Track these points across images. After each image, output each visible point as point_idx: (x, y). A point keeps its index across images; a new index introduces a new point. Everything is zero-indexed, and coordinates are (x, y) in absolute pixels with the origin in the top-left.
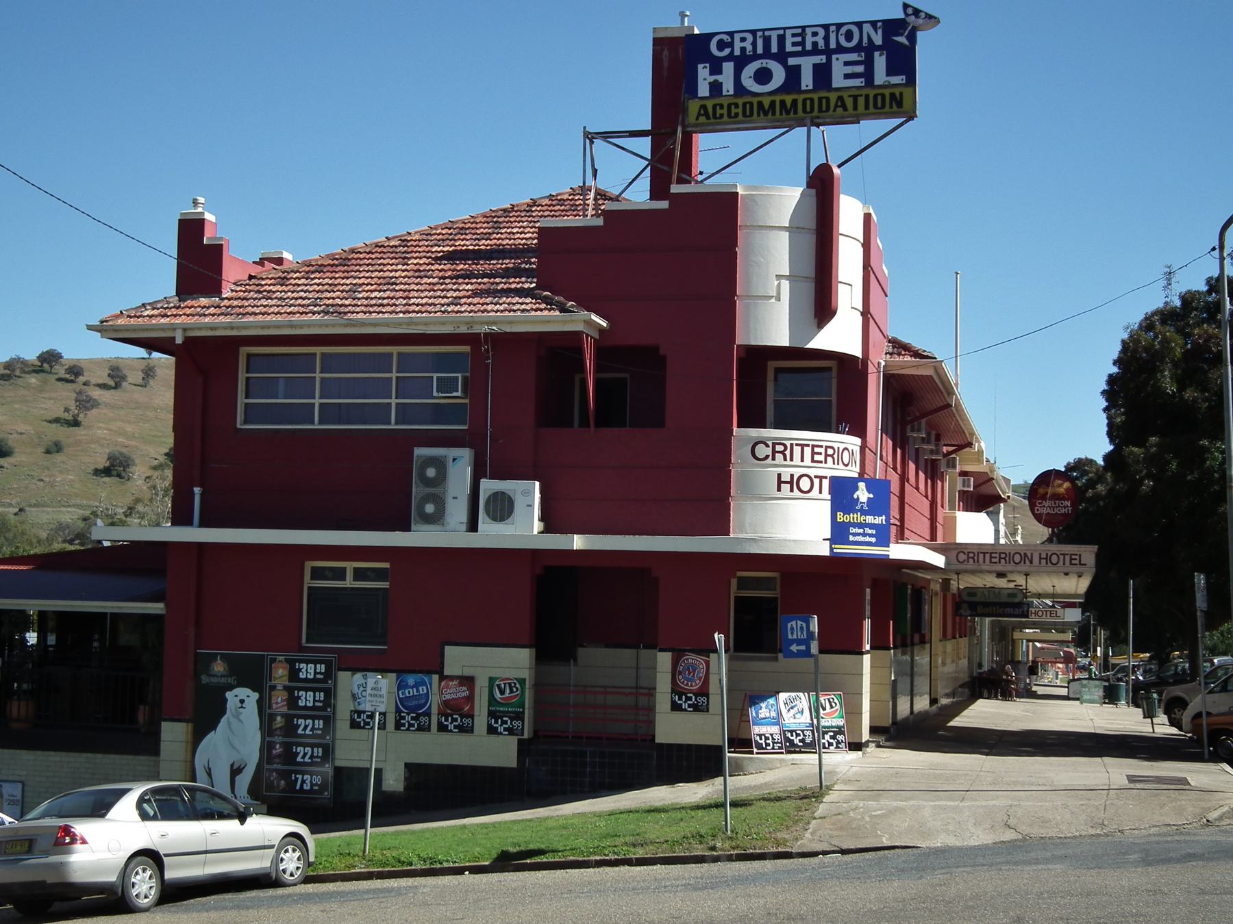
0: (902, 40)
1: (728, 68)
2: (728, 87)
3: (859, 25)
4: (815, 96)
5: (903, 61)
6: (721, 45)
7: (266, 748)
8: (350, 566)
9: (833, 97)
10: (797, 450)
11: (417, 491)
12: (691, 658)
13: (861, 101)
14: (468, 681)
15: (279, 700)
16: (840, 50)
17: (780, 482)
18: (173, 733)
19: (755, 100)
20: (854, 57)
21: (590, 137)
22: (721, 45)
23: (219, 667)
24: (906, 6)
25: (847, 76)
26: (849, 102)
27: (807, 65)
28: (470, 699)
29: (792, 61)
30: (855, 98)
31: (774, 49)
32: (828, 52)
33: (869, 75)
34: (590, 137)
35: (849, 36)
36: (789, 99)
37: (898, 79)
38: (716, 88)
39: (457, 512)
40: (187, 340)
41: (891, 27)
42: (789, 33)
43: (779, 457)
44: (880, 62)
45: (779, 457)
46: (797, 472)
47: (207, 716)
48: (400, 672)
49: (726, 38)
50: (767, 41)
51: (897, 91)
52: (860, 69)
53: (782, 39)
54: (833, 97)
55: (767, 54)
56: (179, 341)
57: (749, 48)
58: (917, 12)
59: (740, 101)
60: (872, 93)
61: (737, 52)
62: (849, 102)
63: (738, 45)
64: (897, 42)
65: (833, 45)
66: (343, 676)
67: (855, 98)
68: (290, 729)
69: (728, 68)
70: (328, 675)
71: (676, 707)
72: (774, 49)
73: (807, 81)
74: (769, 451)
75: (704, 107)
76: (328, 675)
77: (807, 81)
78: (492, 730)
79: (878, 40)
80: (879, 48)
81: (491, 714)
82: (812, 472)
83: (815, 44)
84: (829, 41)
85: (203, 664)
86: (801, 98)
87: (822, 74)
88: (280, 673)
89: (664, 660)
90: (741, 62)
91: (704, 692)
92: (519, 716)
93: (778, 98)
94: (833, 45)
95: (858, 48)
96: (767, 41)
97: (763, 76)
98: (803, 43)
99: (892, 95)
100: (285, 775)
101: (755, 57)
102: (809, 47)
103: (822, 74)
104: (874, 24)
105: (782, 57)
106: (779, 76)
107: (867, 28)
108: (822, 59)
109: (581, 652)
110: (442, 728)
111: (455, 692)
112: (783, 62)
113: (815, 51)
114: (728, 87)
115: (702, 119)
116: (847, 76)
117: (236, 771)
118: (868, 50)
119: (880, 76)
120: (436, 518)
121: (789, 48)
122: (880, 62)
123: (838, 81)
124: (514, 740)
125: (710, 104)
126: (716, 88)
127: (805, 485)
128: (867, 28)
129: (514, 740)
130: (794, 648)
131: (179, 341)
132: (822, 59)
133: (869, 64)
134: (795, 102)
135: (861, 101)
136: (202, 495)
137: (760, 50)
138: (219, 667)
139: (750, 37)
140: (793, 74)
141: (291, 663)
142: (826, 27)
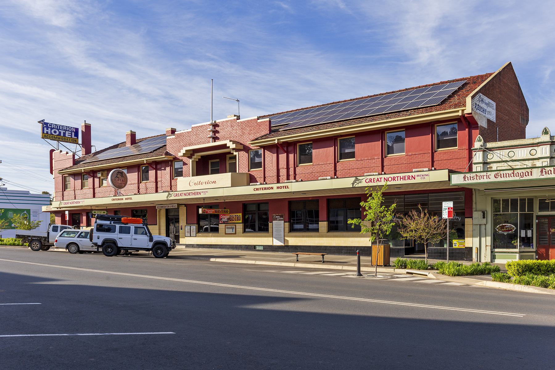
1: (49, 129)
2: (49, 132)
6: (50, 125)
22: (50, 125)
27: (62, 132)
33: (71, 135)
55: (57, 129)
69: (49, 129)
73: (62, 135)
77: (62, 135)
84: (66, 129)
87: (64, 134)
90: (52, 129)
97: (55, 132)
103: (64, 134)
106: (58, 133)
114: (49, 132)
119: (73, 136)
122: (73, 134)
123: (67, 136)
126: (47, 132)
133: (72, 134)
140: (60, 133)
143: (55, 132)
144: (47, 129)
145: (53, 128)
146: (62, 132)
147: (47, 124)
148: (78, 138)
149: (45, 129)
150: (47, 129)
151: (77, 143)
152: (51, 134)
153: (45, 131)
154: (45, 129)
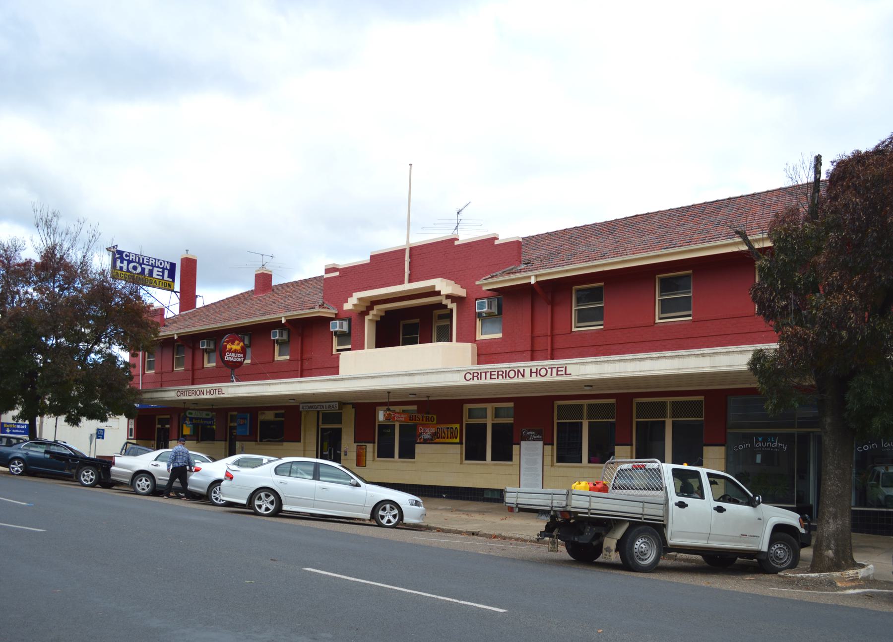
1: (125, 262)
2: (125, 268)
16: (158, 267)
22: (126, 256)
27: (147, 268)
33: (163, 276)
37: (170, 280)
73: (147, 272)
77: (147, 272)
87: (151, 272)
90: (129, 262)
95: (163, 268)
97: (135, 268)
105: (141, 265)
106: (139, 270)
114: (125, 268)
122: (166, 272)
123: (155, 275)
126: (121, 268)
133: (163, 272)
140: (143, 269)
144: (122, 262)
145: (132, 261)
146: (147, 268)
147: (121, 253)
148: (174, 281)
149: (118, 262)
150: (122, 262)
151: (173, 291)
152: (128, 271)
153: (118, 264)
154: (118, 262)
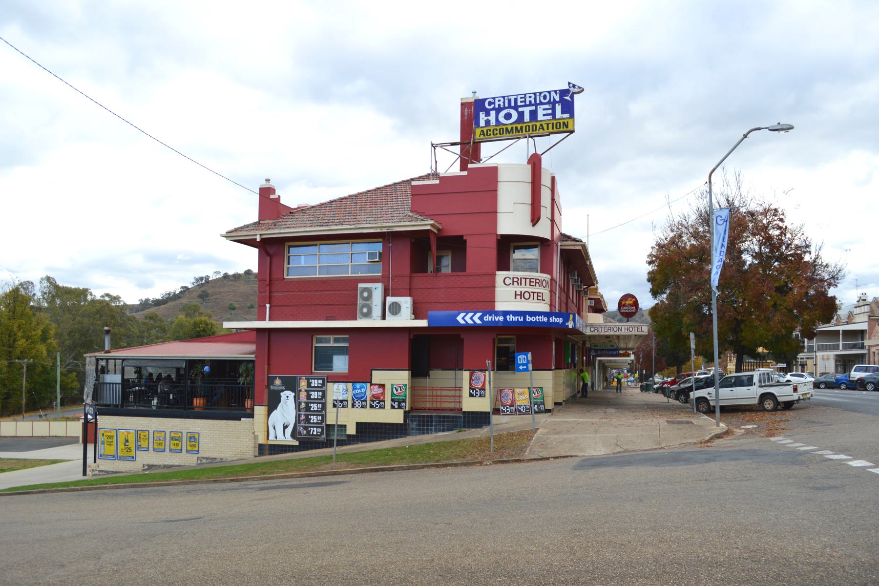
0: (568, 98)
1: (493, 113)
3: (549, 92)
4: (530, 124)
5: (568, 108)
6: (490, 103)
7: (298, 417)
8: (332, 337)
9: (538, 124)
10: (523, 281)
11: (360, 302)
12: (478, 374)
13: (550, 126)
14: (382, 386)
15: (303, 395)
16: (541, 103)
17: (516, 295)
18: (260, 411)
19: (504, 127)
20: (547, 106)
21: (434, 146)
22: (490, 103)
23: (278, 382)
24: (569, 83)
25: (544, 115)
26: (545, 127)
27: (527, 111)
28: (383, 394)
29: (520, 109)
30: (548, 124)
31: (513, 104)
32: (536, 105)
33: (553, 114)
34: (434, 146)
35: (545, 97)
36: (519, 126)
37: (567, 116)
38: (488, 123)
39: (377, 311)
40: (262, 239)
41: (563, 93)
42: (519, 97)
43: (516, 284)
44: (558, 108)
45: (516, 284)
46: (523, 290)
47: (273, 403)
48: (353, 382)
49: (492, 100)
50: (510, 101)
51: (566, 121)
52: (550, 112)
53: (516, 100)
54: (538, 124)
55: (510, 107)
56: (258, 240)
57: (502, 104)
58: (574, 86)
59: (498, 128)
60: (555, 122)
61: (497, 106)
62: (545, 127)
63: (497, 103)
64: (566, 100)
65: (538, 102)
66: (329, 385)
67: (548, 124)
68: (308, 408)
69: (493, 113)
70: (323, 384)
71: (471, 395)
72: (513, 104)
73: (527, 118)
74: (511, 281)
75: (483, 131)
76: (323, 384)
77: (527, 118)
78: (393, 407)
79: (557, 98)
80: (558, 102)
81: (392, 400)
82: (530, 290)
83: (530, 102)
84: (536, 100)
85: (271, 381)
86: (524, 125)
87: (533, 114)
88: (303, 384)
89: (466, 374)
90: (498, 110)
91: (483, 388)
92: (404, 401)
93: (514, 126)
94: (538, 102)
96: (510, 101)
97: (508, 116)
98: (525, 101)
99: (564, 123)
100: (305, 428)
101: (505, 108)
102: (528, 103)
103: (533, 114)
104: (555, 92)
105: (516, 108)
106: (515, 116)
107: (553, 94)
108: (533, 108)
109: (431, 372)
110: (371, 407)
111: (377, 391)
112: (517, 110)
113: (530, 104)
115: (482, 136)
116: (544, 115)
117: (285, 427)
118: (553, 103)
119: (558, 114)
120: (368, 315)
121: (519, 104)
122: (558, 108)
123: (540, 117)
124: (401, 412)
125: (485, 130)
126: (488, 123)
127: (527, 295)
128: (553, 94)
129: (401, 412)
130: (521, 367)
131: (258, 240)
132: (533, 108)
133: (554, 109)
134: (522, 127)
135: (550, 126)
136: (270, 307)
137: (507, 105)
138: (278, 382)
139: (502, 100)
140: (521, 115)
141: (308, 379)
142: (535, 94)
143: (508, 116)
